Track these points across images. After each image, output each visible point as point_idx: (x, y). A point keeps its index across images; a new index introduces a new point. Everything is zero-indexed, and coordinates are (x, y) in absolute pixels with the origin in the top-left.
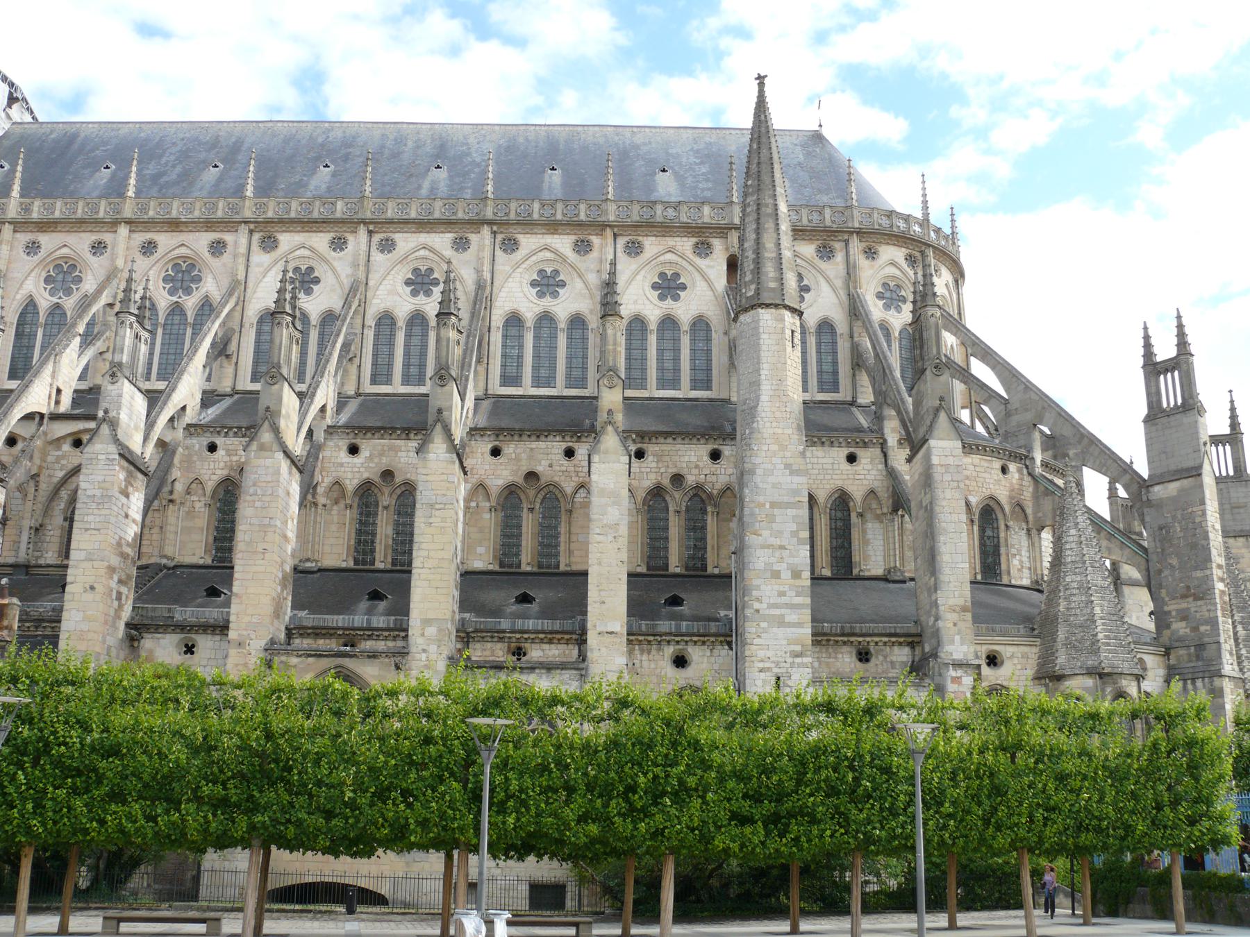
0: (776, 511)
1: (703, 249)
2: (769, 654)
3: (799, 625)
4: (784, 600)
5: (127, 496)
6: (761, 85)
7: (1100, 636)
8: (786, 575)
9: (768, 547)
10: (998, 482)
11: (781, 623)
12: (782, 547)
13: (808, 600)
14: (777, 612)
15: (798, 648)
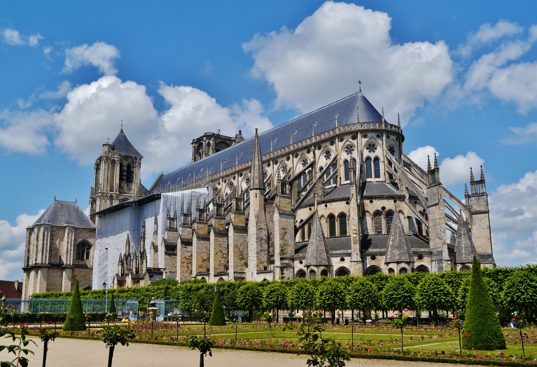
0: (252, 236)
1: (309, 152)
2: (251, 268)
3: (255, 261)
4: (253, 256)
5: (187, 248)
6: (257, 131)
7: (309, 256)
8: (253, 250)
9: (251, 244)
10: (345, 207)
11: (253, 261)
12: (253, 244)
13: (256, 255)
14: (252, 258)
15: (255, 266)
